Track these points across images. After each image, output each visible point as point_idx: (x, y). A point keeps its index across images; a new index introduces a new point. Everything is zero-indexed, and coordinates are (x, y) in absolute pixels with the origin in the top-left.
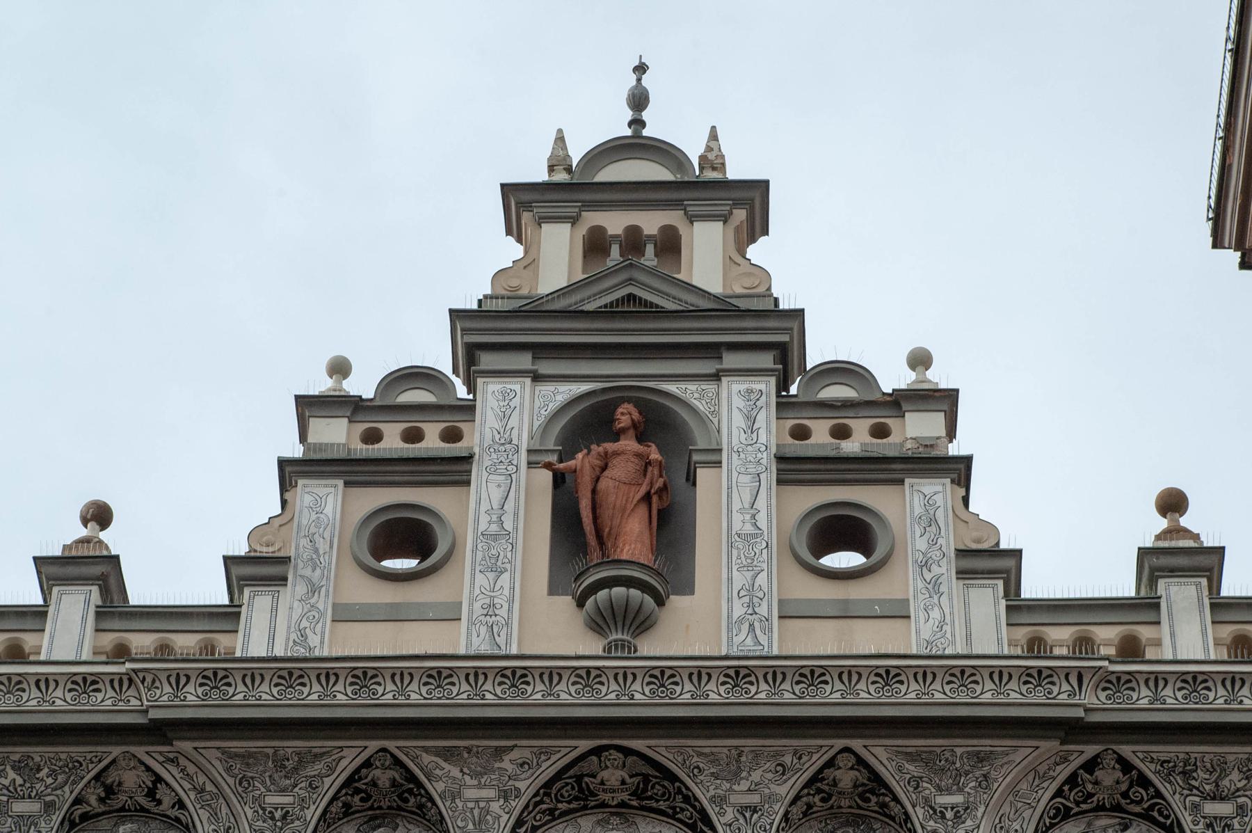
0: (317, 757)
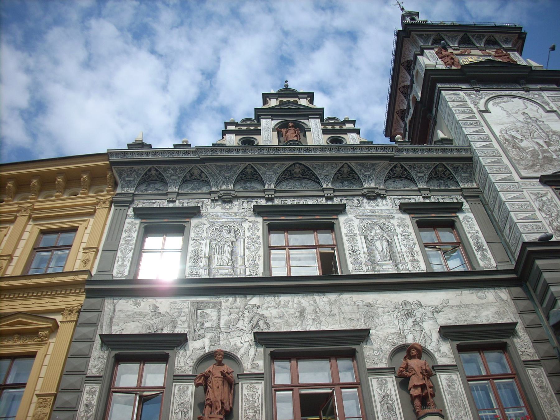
0: (236, 166)
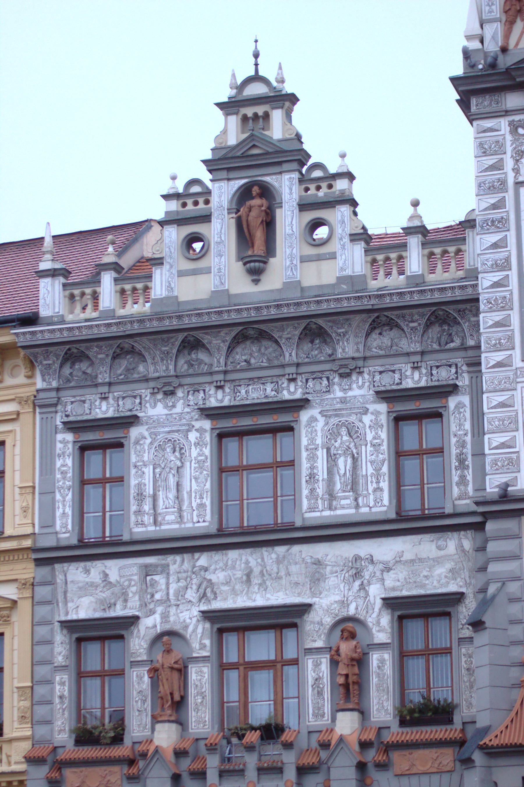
0: (172, 338)
